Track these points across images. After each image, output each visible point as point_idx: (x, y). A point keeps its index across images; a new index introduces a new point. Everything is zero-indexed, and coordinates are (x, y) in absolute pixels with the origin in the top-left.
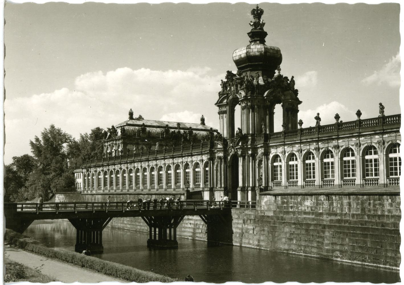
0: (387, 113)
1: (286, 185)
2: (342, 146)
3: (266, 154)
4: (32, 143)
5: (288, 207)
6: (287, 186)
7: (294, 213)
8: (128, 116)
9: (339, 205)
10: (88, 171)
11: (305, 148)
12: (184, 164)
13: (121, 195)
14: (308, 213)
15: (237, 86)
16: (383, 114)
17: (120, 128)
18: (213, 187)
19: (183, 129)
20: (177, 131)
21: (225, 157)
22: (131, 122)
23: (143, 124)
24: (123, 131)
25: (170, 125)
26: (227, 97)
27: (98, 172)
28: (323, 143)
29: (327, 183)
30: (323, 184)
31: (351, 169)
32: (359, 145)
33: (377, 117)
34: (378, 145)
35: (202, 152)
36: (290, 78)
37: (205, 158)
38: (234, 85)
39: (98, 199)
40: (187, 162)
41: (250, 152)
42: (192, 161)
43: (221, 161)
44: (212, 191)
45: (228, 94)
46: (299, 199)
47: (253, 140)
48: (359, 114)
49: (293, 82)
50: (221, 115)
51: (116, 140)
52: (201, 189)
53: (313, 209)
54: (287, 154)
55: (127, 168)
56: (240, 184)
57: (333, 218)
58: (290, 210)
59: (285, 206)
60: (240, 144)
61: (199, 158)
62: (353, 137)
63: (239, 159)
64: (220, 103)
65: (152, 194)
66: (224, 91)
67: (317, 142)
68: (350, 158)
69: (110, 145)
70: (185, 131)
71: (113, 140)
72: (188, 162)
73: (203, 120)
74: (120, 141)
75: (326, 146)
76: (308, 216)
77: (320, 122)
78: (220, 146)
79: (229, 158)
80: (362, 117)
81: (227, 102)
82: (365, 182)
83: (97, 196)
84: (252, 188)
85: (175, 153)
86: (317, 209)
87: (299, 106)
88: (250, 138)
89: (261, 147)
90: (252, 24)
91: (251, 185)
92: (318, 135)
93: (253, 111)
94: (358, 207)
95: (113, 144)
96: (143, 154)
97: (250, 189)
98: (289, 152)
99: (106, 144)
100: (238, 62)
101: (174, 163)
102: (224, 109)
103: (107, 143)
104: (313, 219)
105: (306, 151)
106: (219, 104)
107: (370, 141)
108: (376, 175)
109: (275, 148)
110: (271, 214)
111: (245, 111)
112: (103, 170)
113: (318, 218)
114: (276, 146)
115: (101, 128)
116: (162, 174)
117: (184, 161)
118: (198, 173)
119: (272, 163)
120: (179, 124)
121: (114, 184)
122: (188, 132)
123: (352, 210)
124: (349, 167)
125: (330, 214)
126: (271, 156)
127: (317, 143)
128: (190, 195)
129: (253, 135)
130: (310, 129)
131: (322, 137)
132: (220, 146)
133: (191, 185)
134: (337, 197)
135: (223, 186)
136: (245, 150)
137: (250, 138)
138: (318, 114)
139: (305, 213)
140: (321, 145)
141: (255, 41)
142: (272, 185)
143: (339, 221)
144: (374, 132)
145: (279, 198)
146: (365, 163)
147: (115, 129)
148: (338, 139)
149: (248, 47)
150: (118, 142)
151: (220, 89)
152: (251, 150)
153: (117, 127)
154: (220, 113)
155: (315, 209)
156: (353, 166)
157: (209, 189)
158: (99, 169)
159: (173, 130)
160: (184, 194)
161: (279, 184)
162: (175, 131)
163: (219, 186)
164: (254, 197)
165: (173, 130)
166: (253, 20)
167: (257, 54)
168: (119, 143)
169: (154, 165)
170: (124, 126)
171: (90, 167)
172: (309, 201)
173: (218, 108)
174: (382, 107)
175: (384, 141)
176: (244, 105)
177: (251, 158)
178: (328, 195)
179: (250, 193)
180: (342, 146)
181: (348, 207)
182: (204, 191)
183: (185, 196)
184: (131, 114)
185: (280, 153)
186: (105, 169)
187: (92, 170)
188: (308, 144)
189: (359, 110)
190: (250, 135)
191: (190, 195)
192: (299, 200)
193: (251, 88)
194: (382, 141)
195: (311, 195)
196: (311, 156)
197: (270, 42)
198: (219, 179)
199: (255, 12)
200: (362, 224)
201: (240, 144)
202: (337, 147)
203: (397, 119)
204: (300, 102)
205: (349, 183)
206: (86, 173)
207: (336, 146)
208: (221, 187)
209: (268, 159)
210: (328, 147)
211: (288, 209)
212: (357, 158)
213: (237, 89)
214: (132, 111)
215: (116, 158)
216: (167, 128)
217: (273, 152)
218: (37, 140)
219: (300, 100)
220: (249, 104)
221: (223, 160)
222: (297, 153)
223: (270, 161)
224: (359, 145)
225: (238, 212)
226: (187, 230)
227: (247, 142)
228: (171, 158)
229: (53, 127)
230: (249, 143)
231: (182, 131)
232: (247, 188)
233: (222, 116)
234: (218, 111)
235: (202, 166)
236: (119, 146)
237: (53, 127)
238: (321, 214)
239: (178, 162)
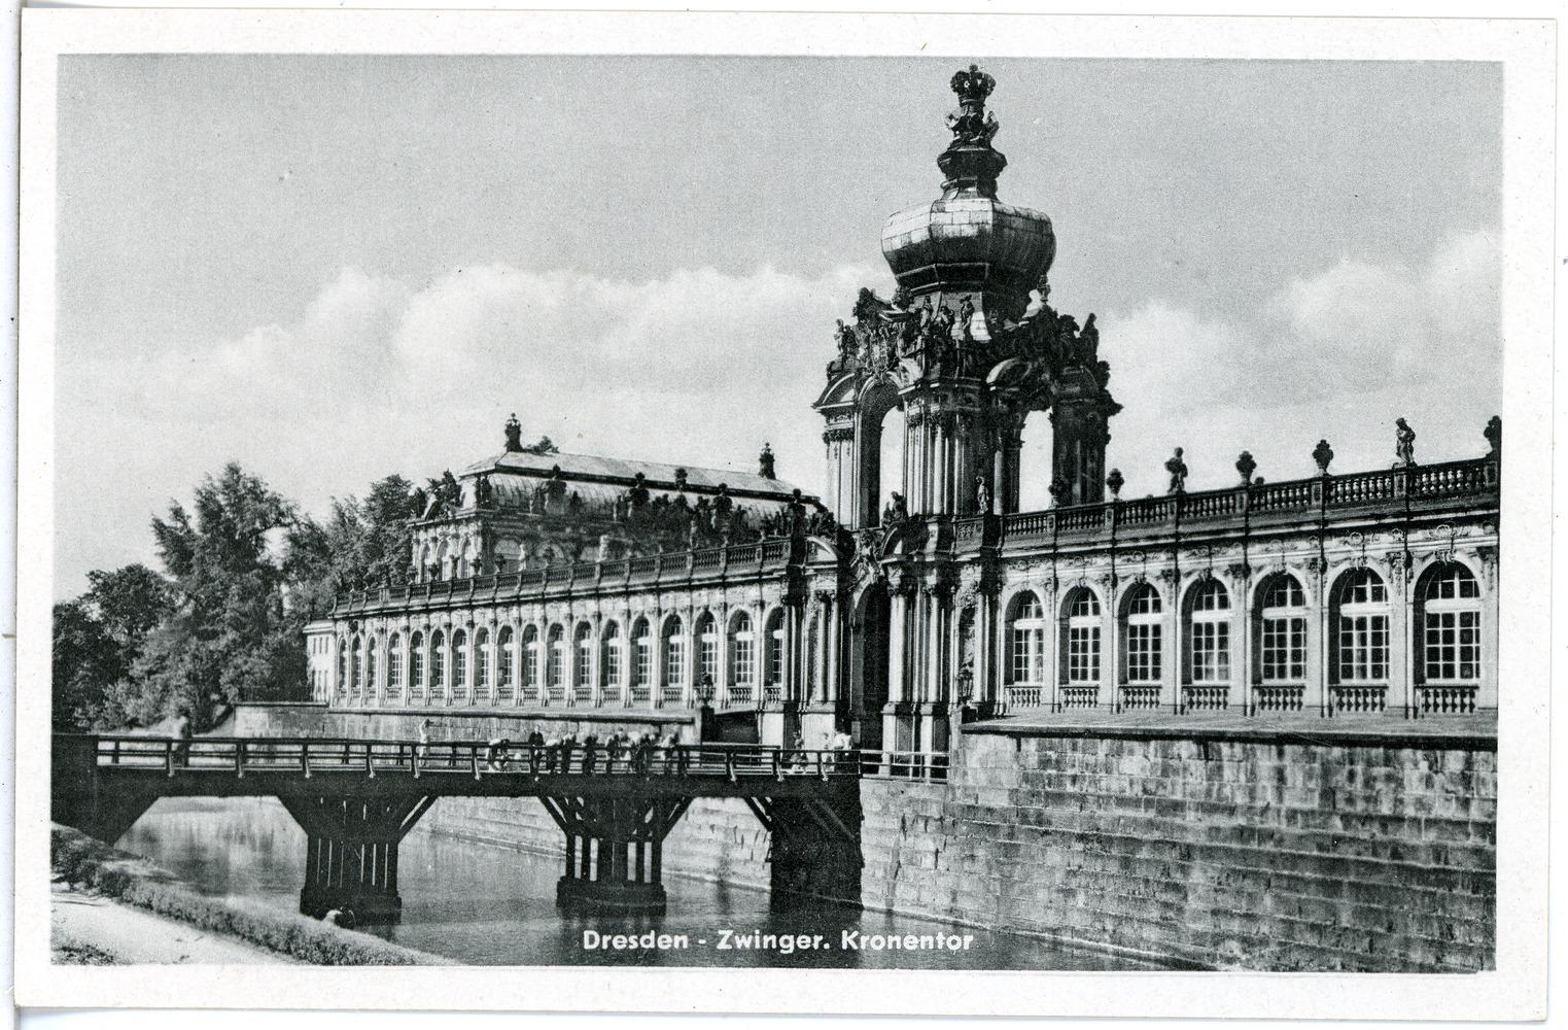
0: (1421, 458)
1: (1179, 702)
2: (1260, 569)
3: (990, 586)
4: (160, 527)
6: (1060, 705)
7: (1082, 799)
8: (505, 439)
9: (1242, 778)
10: (354, 628)
11: (1130, 570)
12: (696, 615)
13: (469, 720)
14: (1135, 803)
15: (891, 340)
16: (1408, 458)
17: (475, 480)
18: (797, 700)
19: (696, 489)
20: (673, 496)
21: (844, 596)
22: (513, 460)
23: (556, 468)
24: (484, 491)
25: (650, 476)
26: (859, 381)
27: (389, 634)
28: (1194, 554)
29: (1202, 698)
30: (1188, 699)
31: (1289, 648)
32: (1319, 565)
33: (1387, 467)
34: (1387, 566)
36: (1081, 322)
37: (774, 594)
38: (881, 340)
39: (389, 727)
40: (706, 608)
41: (932, 580)
43: (828, 609)
44: (792, 713)
45: (859, 371)
46: (1104, 746)
47: (946, 539)
48: (1323, 454)
49: (1091, 332)
50: (833, 445)
51: (458, 522)
52: (753, 707)
53: (1151, 787)
54: (1063, 591)
55: (495, 622)
56: (895, 693)
57: (1222, 821)
58: (1070, 788)
59: (1049, 777)
60: (898, 550)
61: (753, 592)
62: (1300, 535)
63: (894, 600)
65: (577, 719)
66: (845, 359)
67: (1173, 549)
68: (1288, 612)
69: (435, 540)
70: (705, 497)
71: (447, 523)
72: (710, 610)
73: (768, 460)
74: (473, 527)
75: (1202, 567)
76: (1130, 813)
77: (1185, 479)
79: (857, 597)
80: (1336, 468)
81: (855, 400)
82: (1337, 699)
83: (382, 718)
84: (934, 707)
85: (665, 575)
86: (1165, 788)
87: (1112, 420)
88: (934, 528)
89: (972, 562)
90: (953, 123)
91: (932, 697)
92: (1178, 524)
93: (947, 434)
94: (1312, 785)
95: (445, 535)
96: (552, 576)
97: (927, 709)
98: (1072, 585)
99: (422, 535)
100: (902, 260)
102: (844, 423)
103: (426, 531)
104: (1151, 825)
105: (1131, 581)
106: (828, 407)
107: (1360, 554)
108: (1378, 672)
109: (1023, 567)
110: (1001, 801)
111: (920, 431)
112: (407, 629)
113: (1168, 819)
114: (1026, 560)
115: (404, 478)
116: (746, 643)
117: (696, 606)
118: (746, 647)
119: (1010, 621)
120: (681, 473)
122: (715, 500)
123: (1287, 795)
124: (1282, 640)
126: (1005, 597)
127: (1170, 555)
128: (713, 725)
129: (942, 520)
130: (1149, 503)
131: (1191, 534)
133: (721, 691)
134: (1238, 747)
135: (832, 695)
137: (934, 528)
138: (1179, 452)
139: (1122, 802)
140: (1185, 561)
141: (962, 187)
142: (1009, 698)
143: (1242, 833)
144: (1374, 522)
145: (1031, 745)
146: (1340, 629)
147: (454, 481)
148: (1246, 541)
149: (938, 207)
150: (463, 530)
151: (834, 353)
152: (935, 571)
153: (463, 478)
154: (827, 439)
156: (1296, 640)
157: (781, 708)
158: (395, 625)
159: (660, 493)
160: (692, 722)
161: (1032, 696)
162: (666, 496)
163: (818, 694)
164: (942, 740)
165: (660, 493)
167: (970, 231)
168: (466, 534)
169: (589, 614)
170: (486, 473)
171: (363, 616)
172: (1138, 757)
174: (1407, 437)
175: (1408, 553)
176: (914, 410)
177: (934, 601)
178: (1206, 742)
179: (927, 724)
180: (1260, 569)
181: (1275, 783)
182: (763, 713)
184: (513, 432)
187: (371, 626)
188: (1138, 558)
189: (1323, 442)
190: (933, 519)
191: (713, 725)
192: (1101, 756)
193: (941, 350)
194: (1404, 554)
195: (1145, 737)
196: (1150, 599)
197: (1017, 192)
198: (819, 671)
199: (967, 85)
200: (1320, 847)
201: (898, 550)
202: (1242, 570)
203: (1459, 476)
204: (1116, 408)
205: (1353, 700)
206: (346, 637)
208: (825, 700)
209: (994, 607)
210: (1209, 570)
211: (1060, 784)
212: (1313, 613)
213: (892, 355)
214: (515, 421)
215: (457, 585)
216: (639, 485)
217: (1015, 580)
218: (178, 513)
219: (1117, 399)
220: (934, 408)
221: (835, 607)
222: (1101, 585)
223: (1001, 616)
224: (1319, 565)
225: (883, 790)
226: (699, 848)
227: (923, 543)
228: (650, 591)
229: (233, 470)
230: (931, 545)
231: (692, 499)
232: (919, 707)
233: (836, 450)
234: (823, 431)
235: (759, 621)
236: (467, 543)
237: (233, 470)
238: (1177, 807)
239: (675, 609)
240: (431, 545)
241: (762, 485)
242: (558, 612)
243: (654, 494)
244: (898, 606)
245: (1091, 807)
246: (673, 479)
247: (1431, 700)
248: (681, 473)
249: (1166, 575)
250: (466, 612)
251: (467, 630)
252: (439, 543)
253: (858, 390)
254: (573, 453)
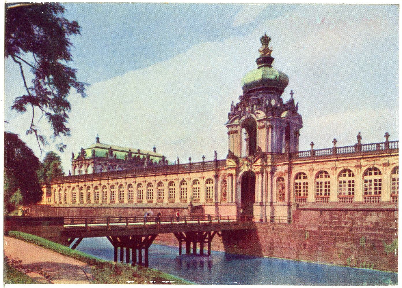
5: (340, 223)
17: (91, 149)
19: (142, 154)
20: (137, 155)
22: (99, 145)
35: (203, 170)
39: (73, 211)
42: (117, 183)
50: (231, 135)
58: (343, 225)
64: (231, 123)
71: (83, 160)
95: (82, 163)
101: (117, 183)
112: (78, 186)
114: (301, 164)
119: (294, 181)
126: (294, 174)
129: (272, 154)
135: (234, 200)
136: (263, 166)
137: (269, 156)
150: (87, 162)
154: (229, 133)
155: (383, 225)
157: (214, 204)
160: (187, 208)
170: (94, 148)
173: (227, 128)
183: (188, 210)
184: (98, 139)
185: (306, 170)
206: (56, 188)
207: (387, 163)
213: (252, 109)
216: (130, 153)
217: (296, 170)
221: (234, 177)
227: (266, 161)
231: (141, 157)
239: (172, 179)
240: (77, 166)
241: (153, 154)
243: (133, 155)
245: (354, 231)
246: (137, 151)
247: (367, 200)
248: (139, 150)
249: (332, 168)
250: (99, 181)
251: (84, 187)
252: (80, 166)
253: (240, 120)
254: (114, 144)
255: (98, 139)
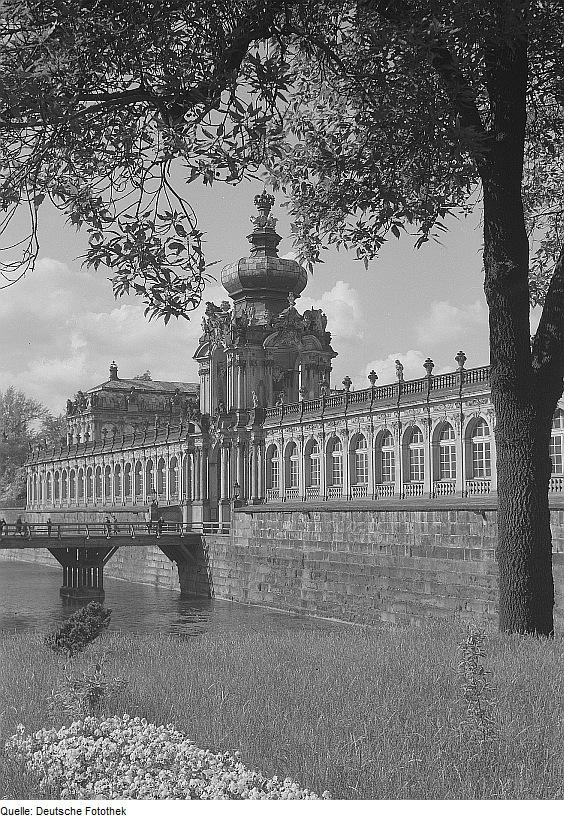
3: (262, 443)
7: (271, 541)
10: (33, 470)
21: (206, 449)
37: (184, 447)
78: (197, 429)
121: (103, 491)
125: (311, 544)
128: (157, 512)
132: (197, 429)
158: (48, 468)
164: (227, 517)
166: (257, 214)
184: (114, 370)
186: (56, 467)
191: (157, 512)
215: (86, 445)
217: (269, 440)
229: (10, 391)
242: (108, 460)
244: (223, 451)
255: (114, 370)
